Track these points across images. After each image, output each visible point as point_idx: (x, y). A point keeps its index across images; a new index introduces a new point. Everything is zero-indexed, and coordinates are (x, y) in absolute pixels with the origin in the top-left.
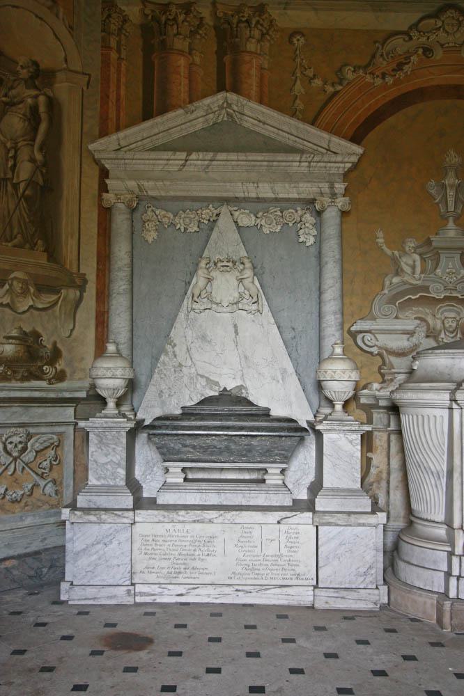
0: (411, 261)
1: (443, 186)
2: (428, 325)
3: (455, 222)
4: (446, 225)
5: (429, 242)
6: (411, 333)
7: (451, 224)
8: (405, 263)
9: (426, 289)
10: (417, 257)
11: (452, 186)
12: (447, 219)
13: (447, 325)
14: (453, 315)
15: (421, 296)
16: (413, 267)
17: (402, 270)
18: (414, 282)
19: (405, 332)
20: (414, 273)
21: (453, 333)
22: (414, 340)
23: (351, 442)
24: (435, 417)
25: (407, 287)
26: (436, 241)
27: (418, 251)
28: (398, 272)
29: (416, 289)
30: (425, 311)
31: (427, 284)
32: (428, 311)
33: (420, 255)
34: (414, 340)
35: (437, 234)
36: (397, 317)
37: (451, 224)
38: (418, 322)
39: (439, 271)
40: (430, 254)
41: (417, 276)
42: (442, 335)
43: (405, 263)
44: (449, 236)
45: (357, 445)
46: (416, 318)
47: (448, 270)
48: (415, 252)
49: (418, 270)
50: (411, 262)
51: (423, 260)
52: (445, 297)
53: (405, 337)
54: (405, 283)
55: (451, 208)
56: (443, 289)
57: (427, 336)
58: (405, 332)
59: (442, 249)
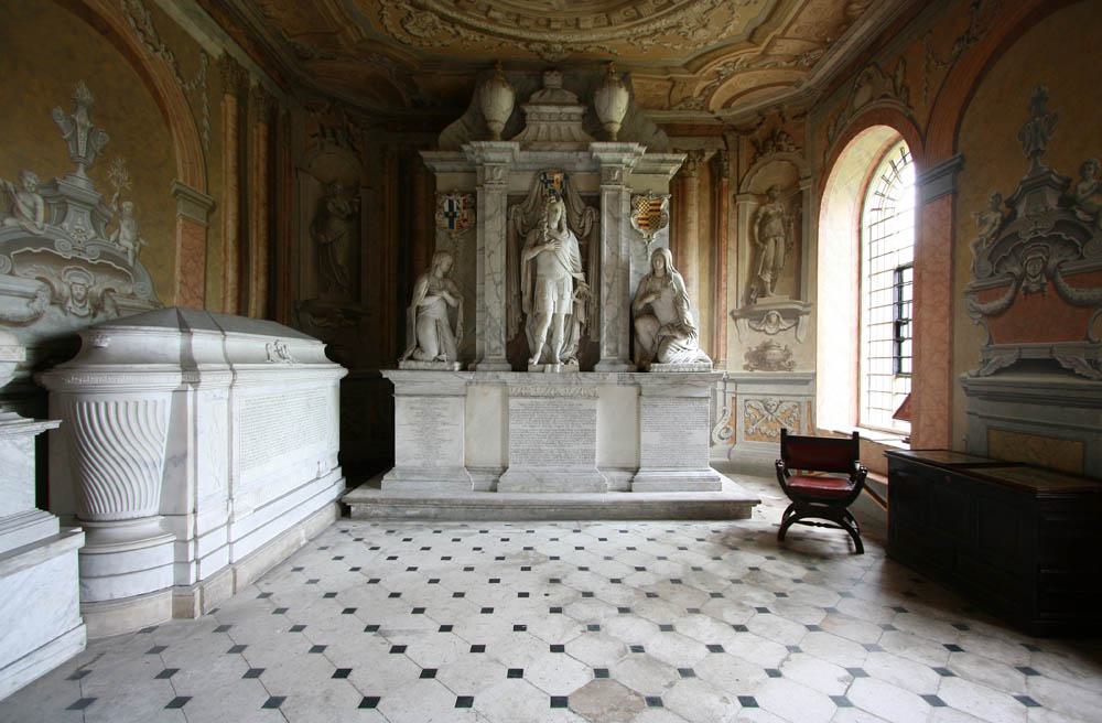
0: (32, 204)
1: (73, 121)
2: (52, 288)
3: (86, 170)
4: (75, 172)
5: (55, 186)
6: (33, 297)
7: (81, 172)
8: (24, 203)
9: (51, 243)
10: (40, 200)
11: (83, 127)
12: (77, 164)
13: (75, 292)
14: (81, 281)
15: (43, 251)
16: (34, 211)
17: (18, 210)
18: (36, 231)
19: (23, 295)
20: (35, 219)
21: (80, 301)
22: (36, 306)
23: (20, 448)
24: (155, 402)
25: (24, 234)
26: (65, 186)
27: (40, 191)
28: (13, 211)
29: (38, 241)
30: (48, 270)
31: (52, 237)
32: (53, 271)
33: (44, 198)
34: (36, 306)
35: (64, 178)
36: (11, 273)
37: (81, 172)
38: (41, 283)
39: (65, 224)
40: (59, 203)
41: (39, 223)
42: (70, 304)
43: (23, 203)
44: (79, 185)
45: (29, 450)
46: (38, 278)
47: (77, 227)
48: (36, 192)
49: (41, 216)
50: (30, 203)
51: (47, 205)
52: (73, 258)
53: (24, 301)
54: (24, 230)
55: (82, 153)
56: (70, 248)
57: (52, 303)
58: (23, 295)
59: (72, 199)
